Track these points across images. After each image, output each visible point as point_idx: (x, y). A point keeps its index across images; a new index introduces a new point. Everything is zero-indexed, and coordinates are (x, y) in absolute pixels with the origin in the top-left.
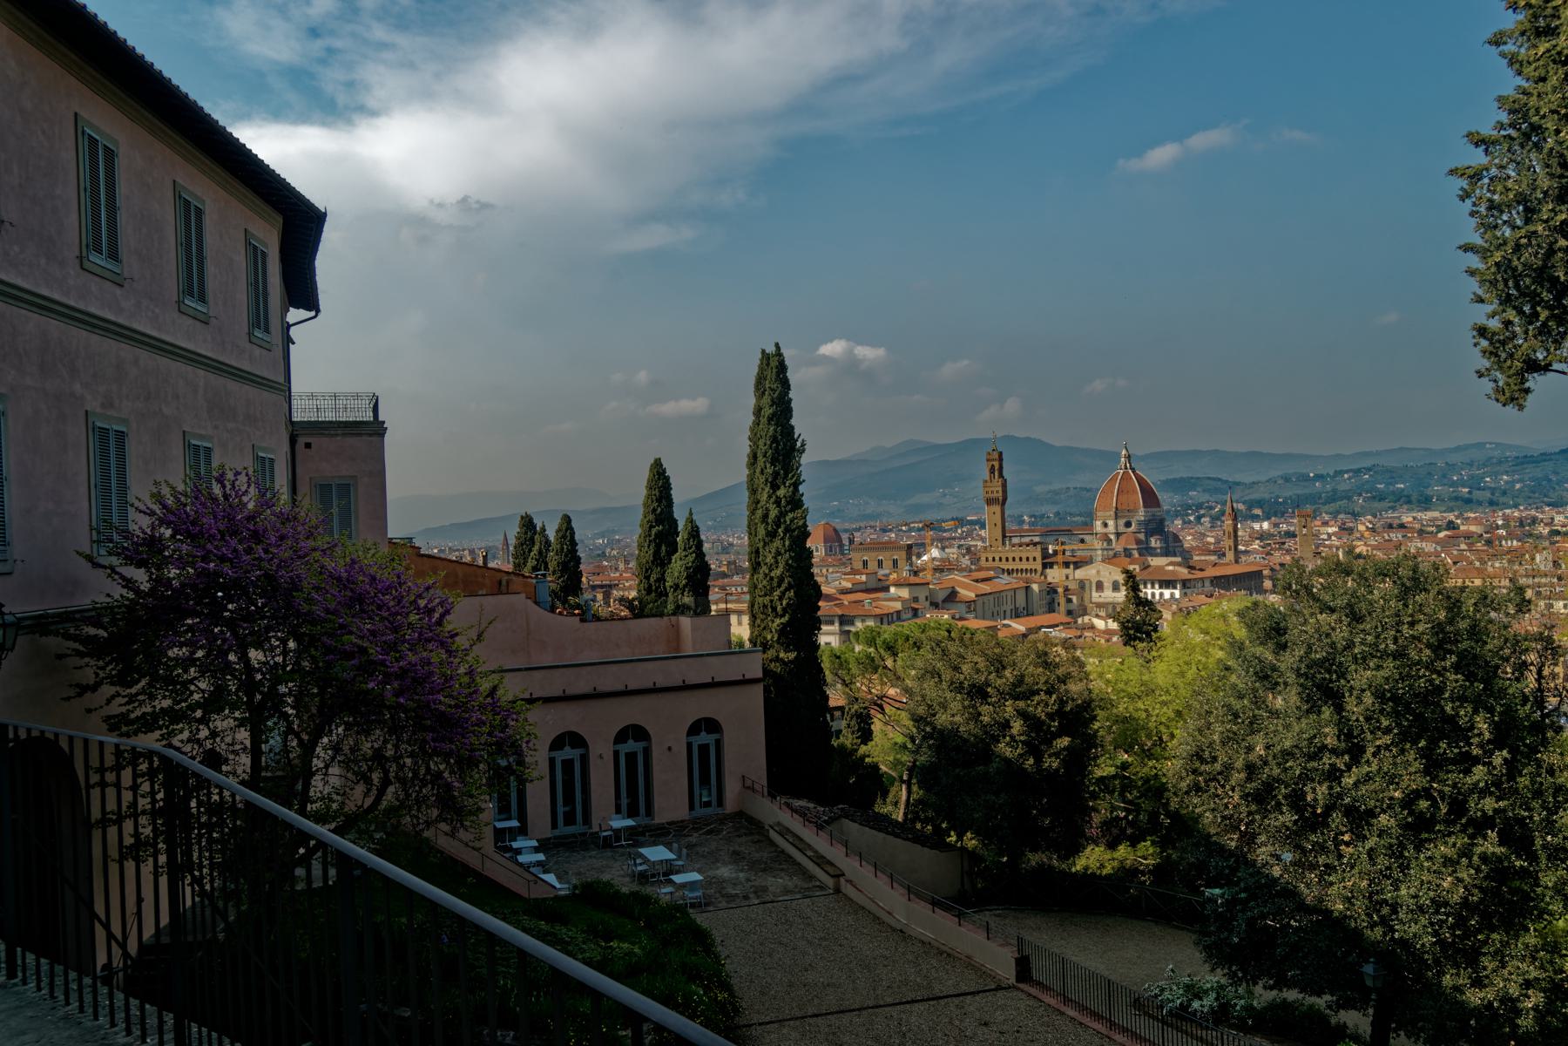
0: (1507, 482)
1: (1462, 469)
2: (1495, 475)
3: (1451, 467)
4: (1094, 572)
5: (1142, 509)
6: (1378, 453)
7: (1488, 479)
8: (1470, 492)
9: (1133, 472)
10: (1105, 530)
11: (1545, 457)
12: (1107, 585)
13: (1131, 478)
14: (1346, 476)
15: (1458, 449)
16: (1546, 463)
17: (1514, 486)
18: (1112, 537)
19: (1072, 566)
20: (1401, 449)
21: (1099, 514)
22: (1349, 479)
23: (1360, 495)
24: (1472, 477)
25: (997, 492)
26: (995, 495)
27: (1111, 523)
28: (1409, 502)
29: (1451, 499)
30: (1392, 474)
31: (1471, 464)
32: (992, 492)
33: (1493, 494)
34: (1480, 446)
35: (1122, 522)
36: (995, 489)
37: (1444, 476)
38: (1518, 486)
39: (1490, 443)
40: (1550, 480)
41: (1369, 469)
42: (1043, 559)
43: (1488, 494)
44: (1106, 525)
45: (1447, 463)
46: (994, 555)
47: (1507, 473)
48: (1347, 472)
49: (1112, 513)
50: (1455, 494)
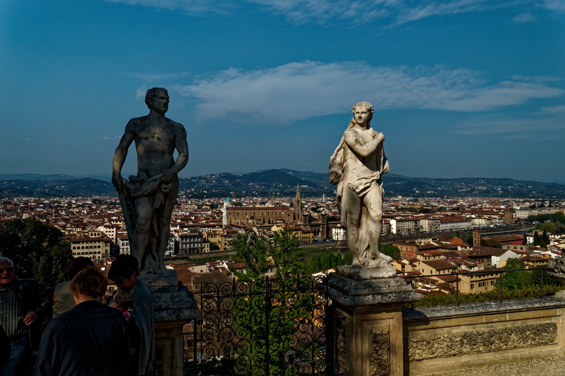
0: (63, 188)
1: (49, 183)
2: (60, 186)
3: (46, 182)
6: (22, 175)
7: (57, 187)
8: (48, 191)
11: (76, 180)
14: (5, 183)
15: (51, 176)
16: (76, 183)
17: (65, 190)
20: (31, 174)
22: (6, 184)
23: (7, 190)
24: (52, 186)
28: (25, 194)
29: (41, 193)
30: (23, 183)
31: (53, 181)
33: (56, 192)
34: (59, 175)
37: (43, 185)
38: (66, 190)
39: (62, 174)
40: (77, 188)
41: (14, 181)
43: (54, 192)
45: (44, 181)
47: (64, 185)
48: (6, 181)
50: (43, 192)
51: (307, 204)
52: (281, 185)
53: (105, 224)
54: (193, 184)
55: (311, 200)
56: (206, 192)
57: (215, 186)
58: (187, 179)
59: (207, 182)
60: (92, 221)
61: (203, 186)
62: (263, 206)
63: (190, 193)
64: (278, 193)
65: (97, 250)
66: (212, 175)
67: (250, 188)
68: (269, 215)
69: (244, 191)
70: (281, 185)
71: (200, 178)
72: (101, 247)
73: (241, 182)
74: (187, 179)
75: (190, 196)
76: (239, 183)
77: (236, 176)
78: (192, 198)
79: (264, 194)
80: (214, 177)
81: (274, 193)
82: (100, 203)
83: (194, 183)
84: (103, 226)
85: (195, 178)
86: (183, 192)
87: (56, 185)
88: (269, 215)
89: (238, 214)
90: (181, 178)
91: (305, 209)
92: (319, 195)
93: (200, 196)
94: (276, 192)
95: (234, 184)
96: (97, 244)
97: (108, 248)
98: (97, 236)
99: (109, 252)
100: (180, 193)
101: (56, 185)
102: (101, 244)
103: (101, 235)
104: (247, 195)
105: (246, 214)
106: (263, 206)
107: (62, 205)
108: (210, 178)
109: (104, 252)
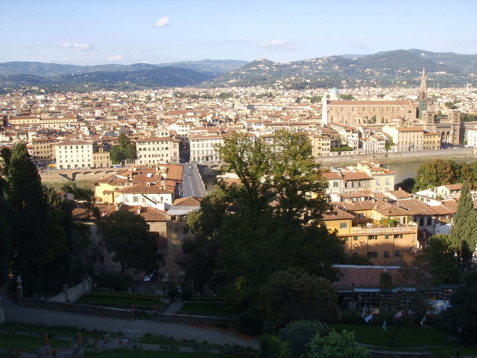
7: (138, 78)
51: (441, 98)
52: (409, 71)
53: (178, 122)
54: (294, 71)
55: (448, 92)
56: (308, 81)
57: (321, 74)
58: (285, 66)
59: (311, 68)
60: (165, 117)
61: (305, 73)
62: (380, 99)
63: (288, 83)
64: (404, 83)
65: (165, 152)
66: (318, 59)
67: (367, 75)
68: (382, 112)
69: (359, 79)
70: (409, 71)
71: (303, 63)
72: (169, 149)
73: (356, 67)
74: (286, 65)
75: (288, 86)
76: (353, 69)
77: (348, 60)
78: (291, 88)
79: (385, 84)
80: (321, 61)
81: (398, 82)
82: (182, 96)
83: (295, 70)
84: (176, 124)
85: (296, 63)
86: (280, 82)
87: (137, 77)
88: (382, 112)
89: (342, 109)
90: (279, 63)
91: (437, 103)
92: (460, 84)
93: (301, 87)
94: (401, 82)
95: (347, 71)
96: (165, 145)
97: (177, 150)
98: (165, 136)
99: (178, 155)
100: (276, 83)
101: (137, 77)
102: (170, 145)
103: (169, 135)
104: (362, 85)
105: (353, 110)
106: (380, 99)
107: (140, 99)
108: (315, 62)
109: (173, 155)
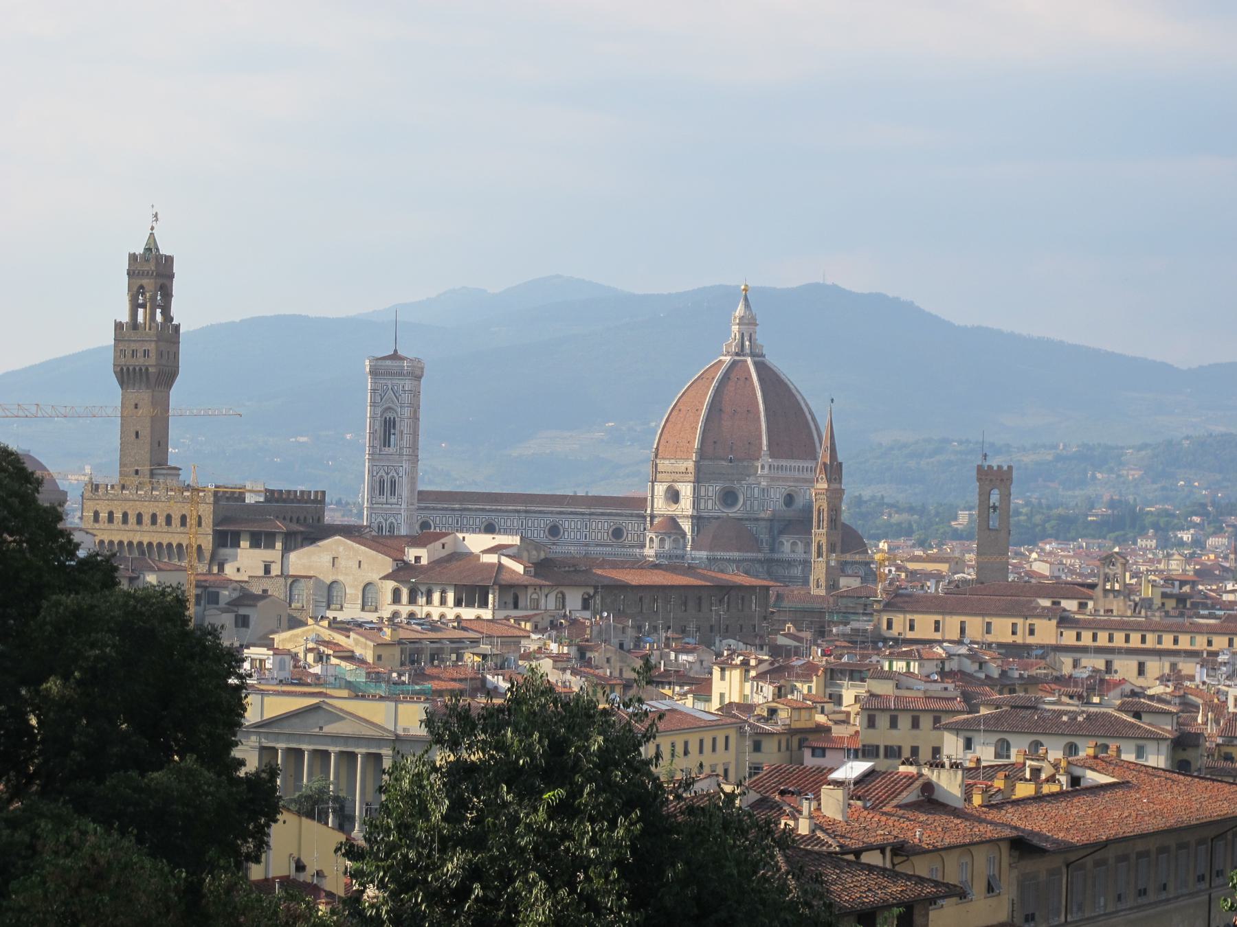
4: (326, 559)
5: (766, 460)
9: (756, 364)
10: (672, 510)
12: (353, 592)
13: (748, 378)
18: (686, 526)
19: (279, 545)
21: (663, 465)
25: (146, 353)
26: (140, 361)
27: (686, 490)
32: (134, 353)
35: (713, 490)
36: (141, 348)
42: (215, 524)
44: (674, 496)
46: (127, 507)
49: (690, 465)
